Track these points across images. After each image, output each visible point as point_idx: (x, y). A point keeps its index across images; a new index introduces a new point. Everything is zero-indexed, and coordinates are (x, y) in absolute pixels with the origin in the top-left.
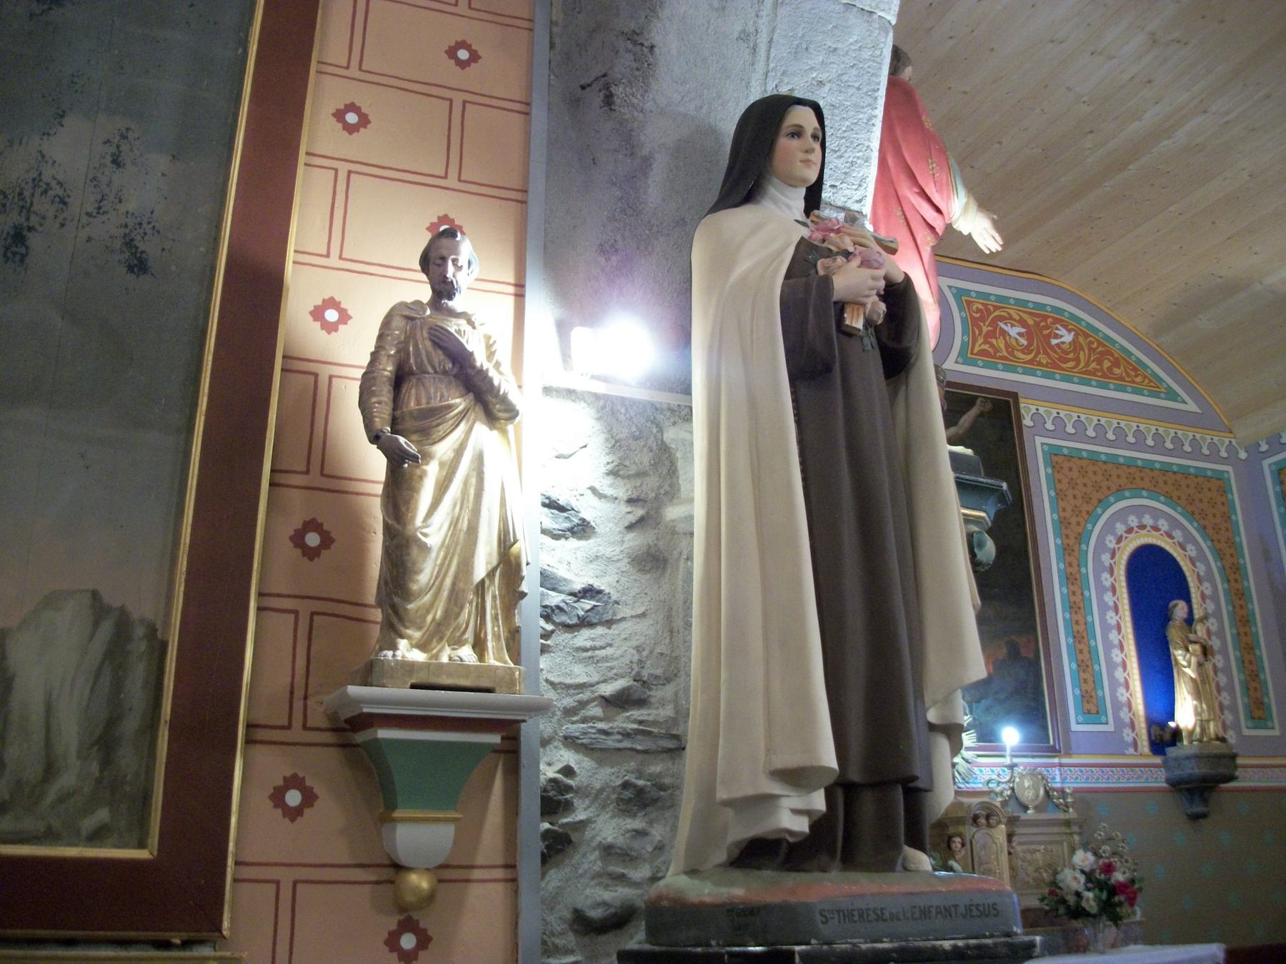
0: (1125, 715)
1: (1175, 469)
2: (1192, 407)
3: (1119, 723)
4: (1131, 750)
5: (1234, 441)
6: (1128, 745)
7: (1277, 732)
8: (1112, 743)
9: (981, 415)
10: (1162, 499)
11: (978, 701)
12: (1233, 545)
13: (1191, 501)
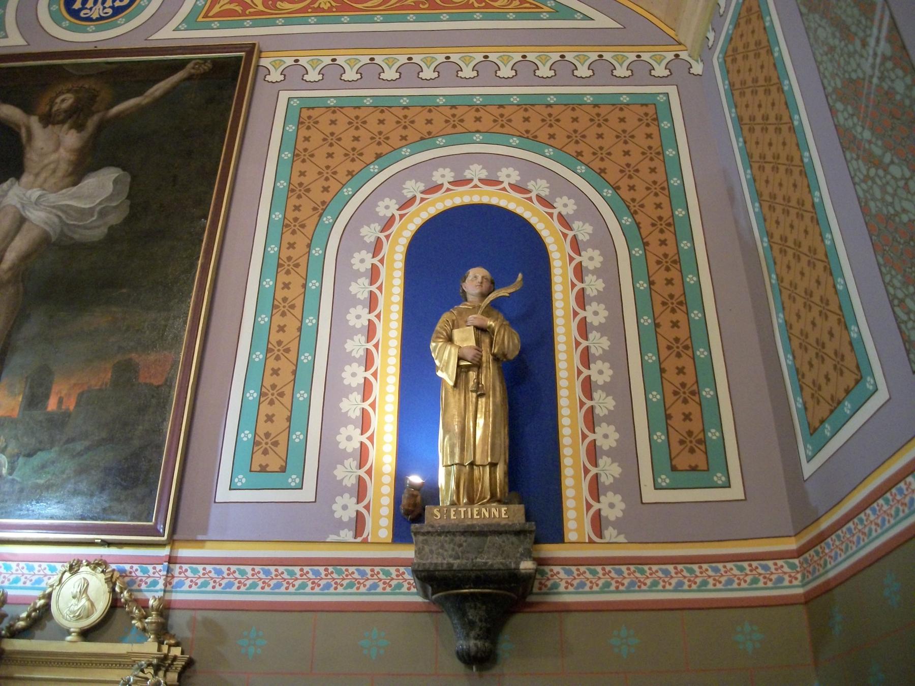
0: (347, 473)
1: (552, 100)
2: (602, 21)
3: (327, 487)
4: (347, 535)
5: (684, 55)
6: (340, 525)
7: (736, 492)
8: (311, 523)
9: (190, 78)
10: (515, 141)
11: (30, 455)
12: (666, 192)
13: (577, 137)
